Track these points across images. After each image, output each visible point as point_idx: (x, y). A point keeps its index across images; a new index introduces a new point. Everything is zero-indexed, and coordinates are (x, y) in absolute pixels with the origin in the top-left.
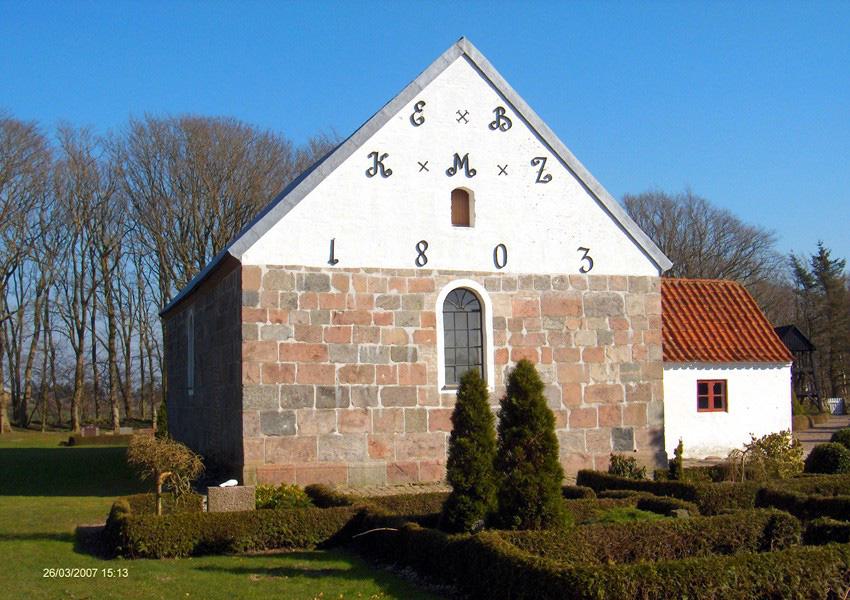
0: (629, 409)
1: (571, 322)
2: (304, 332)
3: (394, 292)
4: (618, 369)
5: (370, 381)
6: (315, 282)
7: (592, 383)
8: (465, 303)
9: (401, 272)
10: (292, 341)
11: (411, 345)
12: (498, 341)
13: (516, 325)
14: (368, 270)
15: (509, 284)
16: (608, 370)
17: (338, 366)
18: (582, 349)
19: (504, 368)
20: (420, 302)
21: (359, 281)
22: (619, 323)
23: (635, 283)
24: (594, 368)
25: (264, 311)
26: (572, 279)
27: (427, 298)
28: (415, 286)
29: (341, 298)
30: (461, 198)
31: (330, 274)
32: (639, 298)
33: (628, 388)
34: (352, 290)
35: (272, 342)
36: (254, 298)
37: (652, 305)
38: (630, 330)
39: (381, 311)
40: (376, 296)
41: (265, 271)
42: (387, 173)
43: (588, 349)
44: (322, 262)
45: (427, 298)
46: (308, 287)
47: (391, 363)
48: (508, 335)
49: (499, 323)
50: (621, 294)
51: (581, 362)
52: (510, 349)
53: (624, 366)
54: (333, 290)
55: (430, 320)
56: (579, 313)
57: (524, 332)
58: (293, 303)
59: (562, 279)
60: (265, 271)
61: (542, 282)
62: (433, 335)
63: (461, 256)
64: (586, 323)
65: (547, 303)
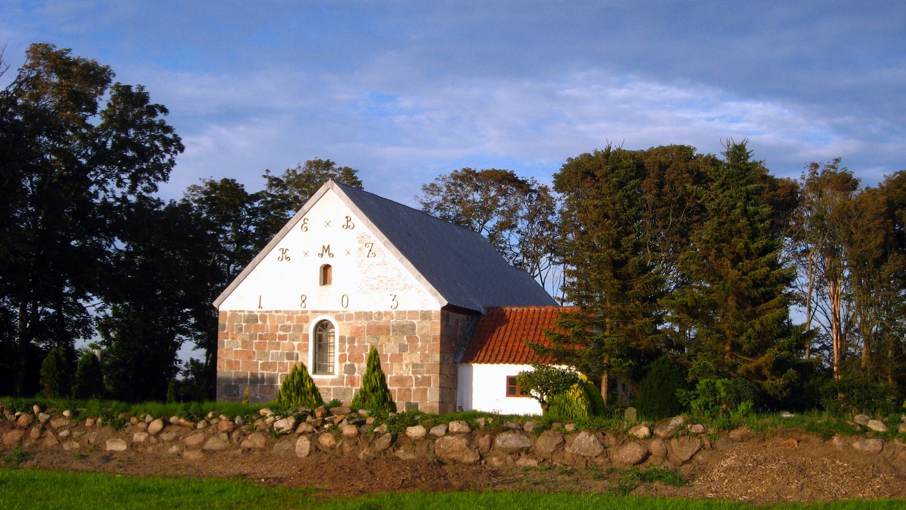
0: (416, 391)
1: (383, 339)
2: (245, 344)
3: (289, 323)
4: (410, 367)
5: (275, 370)
6: (252, 319)
7: (394, 375)
8: (323, 327)
9: (293, 312)
10: (239, 349)
11: (296, 351)
12: (342, 349)
13: (352, 340)
14: (277, 312)
15: (349, 317)
16: (404, 367)
17: (260, 362)
18: (389, 354)
19: (344, 365)
20: (301, 329)
21: (272, 317)
22: (412, 339)
23: (425, 315)
24: (396, 366)
25: (227, 334)
26: (386, 313)
27: (305, 325)
28: (300, 320)
29: (263, 326)
30: (326, 268)
31: (258, 314)
32: (427, 323)
33: (417, 378)
34: (268, 323)
35: (231, 349)
36: (224, 327)
37: (435, 328)
38: (420, 343)
39: (282, 333)
40: (280, 325)
41: (229, 313)
42: (288, 259)
43: (392, 355)
44: (255, 309)
45: (305, 325)
46: (247, 321)
47: (286, 361)
48: (347, 346)
49: (342, 339)
50: (415, 321)
51: (388, 362)
52: (348, 354)
53: (415, 366)
54: (260, 323)
55: (306, 337)
56: (388, 333)
57: (356, 344)
58: (241, 329)
59: (379, 313)
60: (229, 313)
61: (368, 315)
62: (307, 346)
63: (324, 302)
64: (392, 339)
65: (370, 327)
